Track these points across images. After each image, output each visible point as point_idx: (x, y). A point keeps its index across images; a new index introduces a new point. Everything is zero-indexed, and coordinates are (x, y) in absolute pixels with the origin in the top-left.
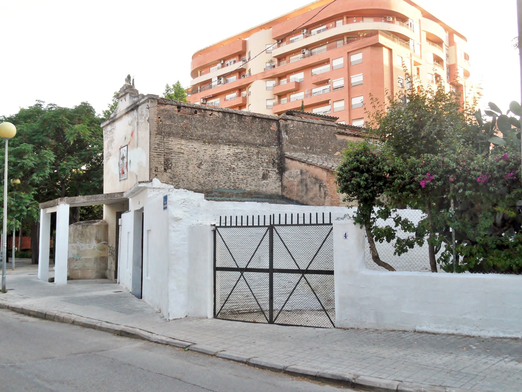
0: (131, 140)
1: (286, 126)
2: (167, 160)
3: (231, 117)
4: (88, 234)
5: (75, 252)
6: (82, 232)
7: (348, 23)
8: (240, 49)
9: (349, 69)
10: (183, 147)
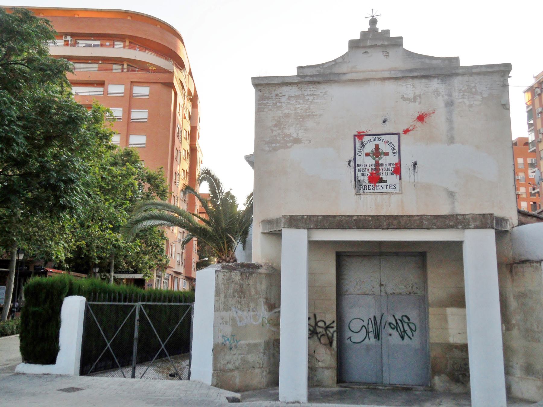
4: (253, 292)
5: (228, 330)
6: (241, 286)
7: (130, 48)
9: (130, 102)
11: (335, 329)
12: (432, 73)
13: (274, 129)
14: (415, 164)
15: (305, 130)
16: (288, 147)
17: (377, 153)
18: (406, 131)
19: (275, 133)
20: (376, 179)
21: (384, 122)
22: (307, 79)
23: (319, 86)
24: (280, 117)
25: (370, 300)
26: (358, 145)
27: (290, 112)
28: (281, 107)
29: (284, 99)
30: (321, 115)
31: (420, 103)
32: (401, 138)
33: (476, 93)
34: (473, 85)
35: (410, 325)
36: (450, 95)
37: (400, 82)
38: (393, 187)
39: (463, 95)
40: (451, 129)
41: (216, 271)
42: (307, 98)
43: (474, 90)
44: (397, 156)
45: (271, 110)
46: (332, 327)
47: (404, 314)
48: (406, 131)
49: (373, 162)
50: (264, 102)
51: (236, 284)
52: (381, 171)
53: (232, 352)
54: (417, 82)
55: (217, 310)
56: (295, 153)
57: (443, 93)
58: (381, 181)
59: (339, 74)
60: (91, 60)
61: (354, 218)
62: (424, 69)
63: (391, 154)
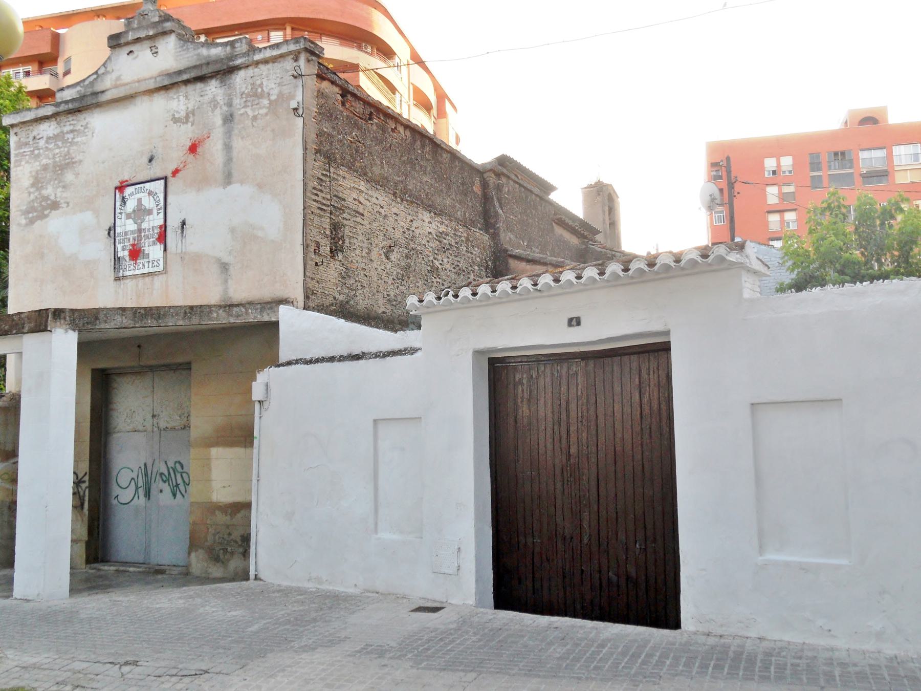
0: (185, 164)
1: (499, 188)
2: (336, 227)
3: (423, 146)
8: (46, 49)
10: (362, 200)
11: (87, 484)
12: (205, 71)
13: (32, 190)
14: (183, 223)
16: (46, 216)
18: (175, 172)
19: (32, 197)
21: (150, 161)
23: (81, 116)
25: (140, 438)
28: (38, 156)
29: (42, 143)
30: (81, 161)
31: (192, 125)
32: (169, 185)
33: (261, 96)
34: (258, 82)
35: (184, 475)
36: (230, 105)
37: (172, 93)
38: (156, 263)
39: (246, 101)
40: (229, 160)
42: (67, 136)
43: (259, 90)
44: (162, 215)
45: (27, 162)
46: (84, 482)
47: (179, 459)
50: (22, 151)
57: (221, 103)
63: (155, 212)
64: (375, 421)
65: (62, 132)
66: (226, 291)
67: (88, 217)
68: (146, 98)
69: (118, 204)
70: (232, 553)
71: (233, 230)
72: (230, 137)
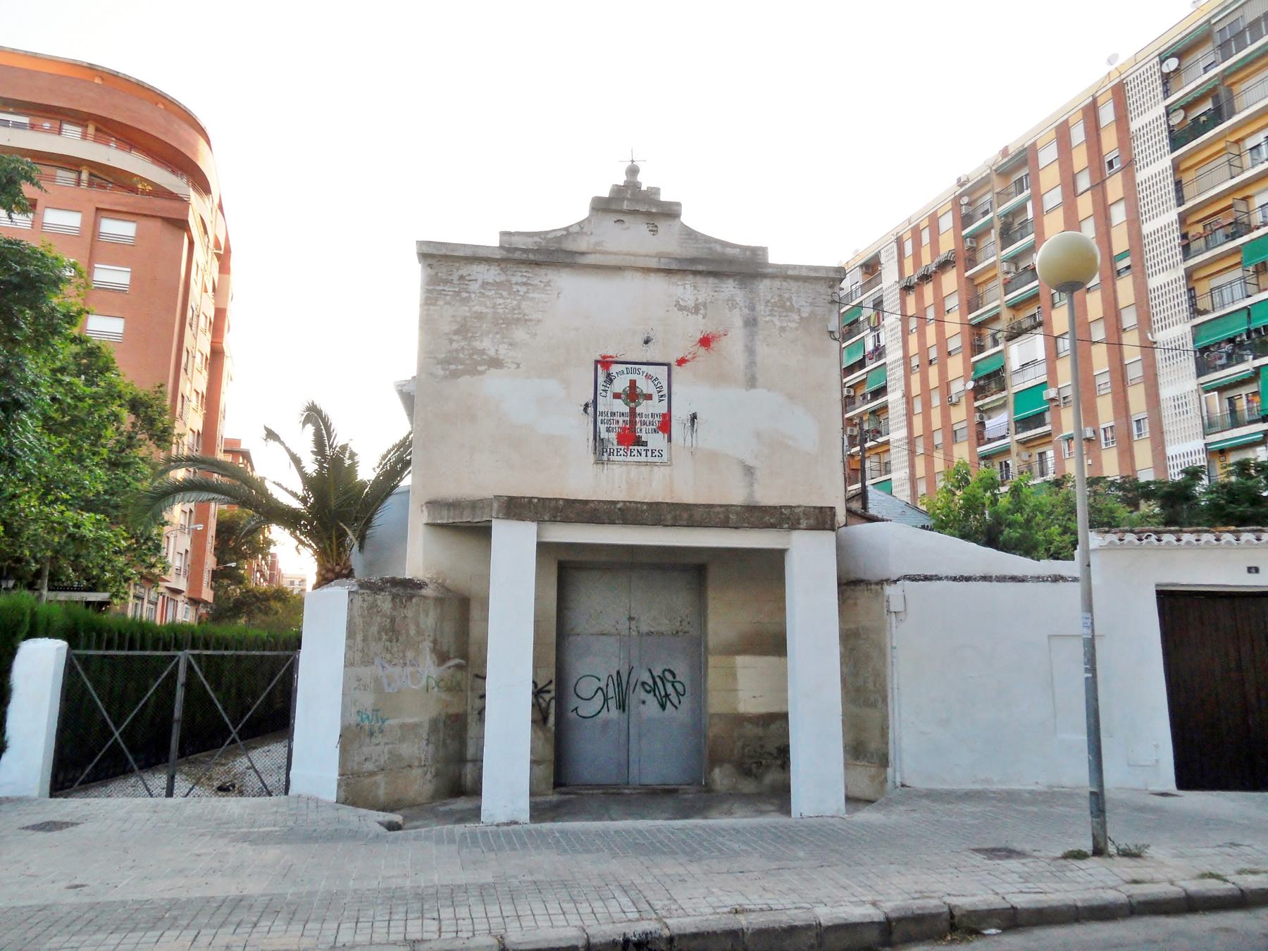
4: (412, 632)
5: (368, 700)
6: (393, 620)
7: (96, 140)
11: (553, 694)
12: (725, 268)
13: (455, 337)
14: (694, 417)
15: (511, 344)
17: (633, 394)
18: (681, 362)
19: (455, 345)
20: (630, 438)
21: (646, 342)
22: (517, 255)
23: (537, 269)
24: (465, 318)
26: (601, 379)
27: (485, 310)
28: (468, 300)
29: (474, 287)
30: (539, 321)
31: (704, 317)
33: (791, 309)
34: (787, 296)
36: (753, 309)
37: (675, 279)
40: (752, 364)
41: (350, 593)
42: (515, 288)
44: (665, 403)
45: (449, 303)
46: (549, 692)
47: (665, 667)
48: (681, 362)
49: (627, 410)
51: (385, 616)
52: (638, 426)
53: (374, 741)
54: (700, 280)
55: (349, 663)
56: (493, 384)
58: (638, 442)
59: (573, 253)
60: (69, 164)
61: (619, 506)
62: (712, 261)
63: (656, 397)
64: (1049, 636)
65: (509, 281)
66: (751, 494)
67: (552, 386)
68: (638, 275)
69: (601, 379)
70: (768, 767)
71: (758, 435)
72: (753, 340)
